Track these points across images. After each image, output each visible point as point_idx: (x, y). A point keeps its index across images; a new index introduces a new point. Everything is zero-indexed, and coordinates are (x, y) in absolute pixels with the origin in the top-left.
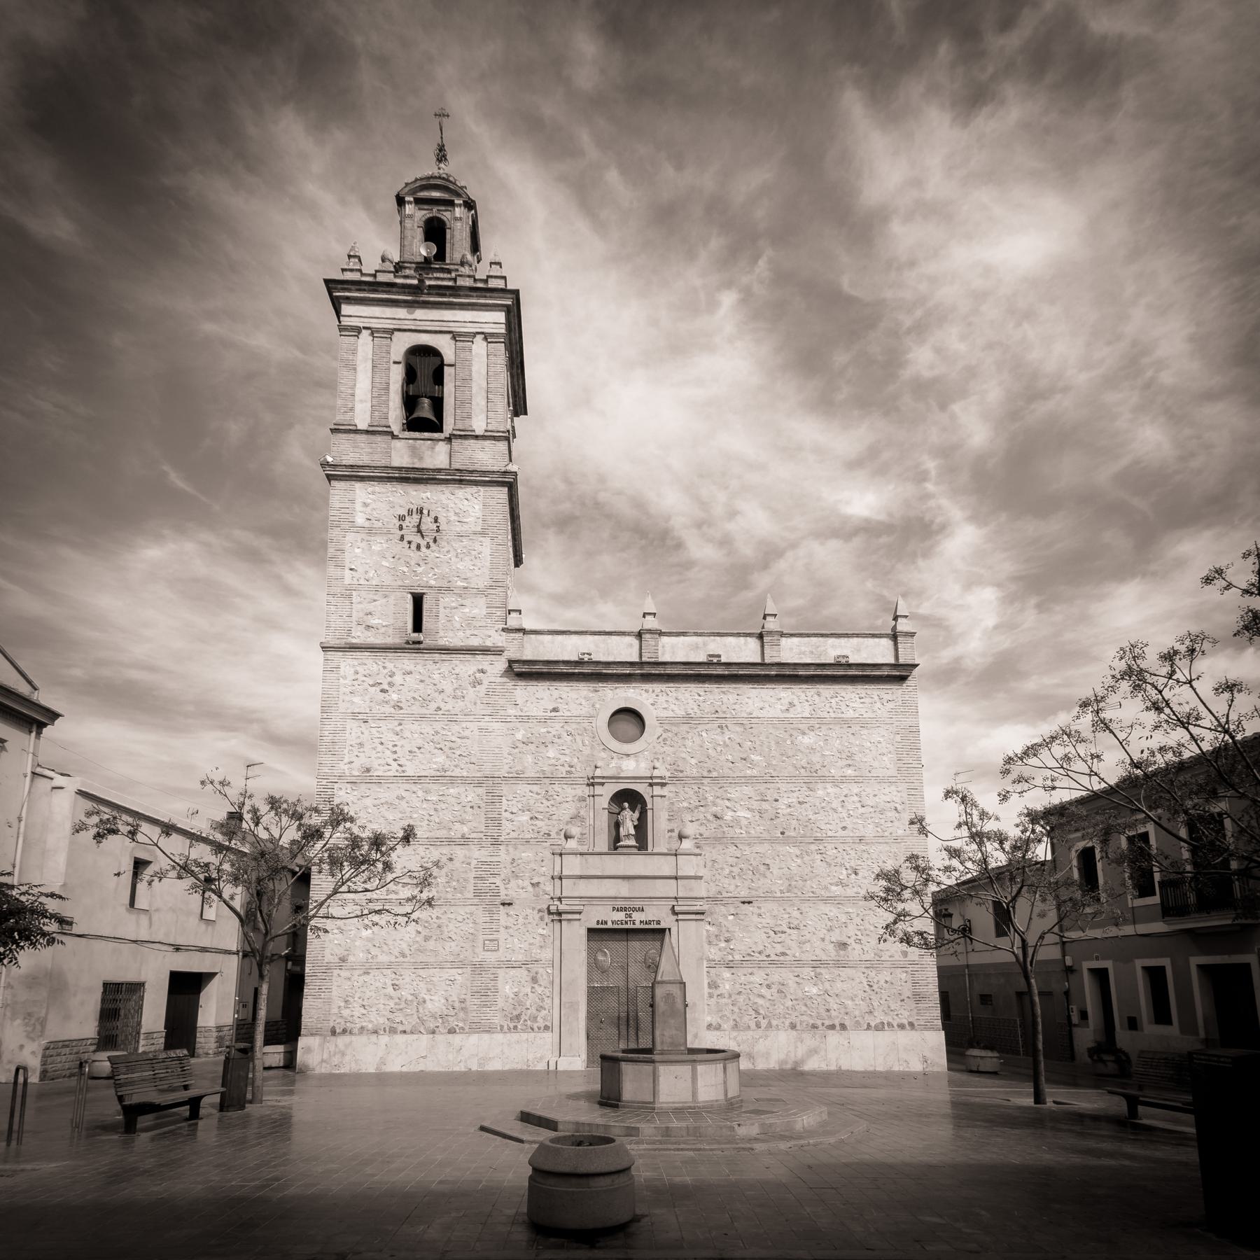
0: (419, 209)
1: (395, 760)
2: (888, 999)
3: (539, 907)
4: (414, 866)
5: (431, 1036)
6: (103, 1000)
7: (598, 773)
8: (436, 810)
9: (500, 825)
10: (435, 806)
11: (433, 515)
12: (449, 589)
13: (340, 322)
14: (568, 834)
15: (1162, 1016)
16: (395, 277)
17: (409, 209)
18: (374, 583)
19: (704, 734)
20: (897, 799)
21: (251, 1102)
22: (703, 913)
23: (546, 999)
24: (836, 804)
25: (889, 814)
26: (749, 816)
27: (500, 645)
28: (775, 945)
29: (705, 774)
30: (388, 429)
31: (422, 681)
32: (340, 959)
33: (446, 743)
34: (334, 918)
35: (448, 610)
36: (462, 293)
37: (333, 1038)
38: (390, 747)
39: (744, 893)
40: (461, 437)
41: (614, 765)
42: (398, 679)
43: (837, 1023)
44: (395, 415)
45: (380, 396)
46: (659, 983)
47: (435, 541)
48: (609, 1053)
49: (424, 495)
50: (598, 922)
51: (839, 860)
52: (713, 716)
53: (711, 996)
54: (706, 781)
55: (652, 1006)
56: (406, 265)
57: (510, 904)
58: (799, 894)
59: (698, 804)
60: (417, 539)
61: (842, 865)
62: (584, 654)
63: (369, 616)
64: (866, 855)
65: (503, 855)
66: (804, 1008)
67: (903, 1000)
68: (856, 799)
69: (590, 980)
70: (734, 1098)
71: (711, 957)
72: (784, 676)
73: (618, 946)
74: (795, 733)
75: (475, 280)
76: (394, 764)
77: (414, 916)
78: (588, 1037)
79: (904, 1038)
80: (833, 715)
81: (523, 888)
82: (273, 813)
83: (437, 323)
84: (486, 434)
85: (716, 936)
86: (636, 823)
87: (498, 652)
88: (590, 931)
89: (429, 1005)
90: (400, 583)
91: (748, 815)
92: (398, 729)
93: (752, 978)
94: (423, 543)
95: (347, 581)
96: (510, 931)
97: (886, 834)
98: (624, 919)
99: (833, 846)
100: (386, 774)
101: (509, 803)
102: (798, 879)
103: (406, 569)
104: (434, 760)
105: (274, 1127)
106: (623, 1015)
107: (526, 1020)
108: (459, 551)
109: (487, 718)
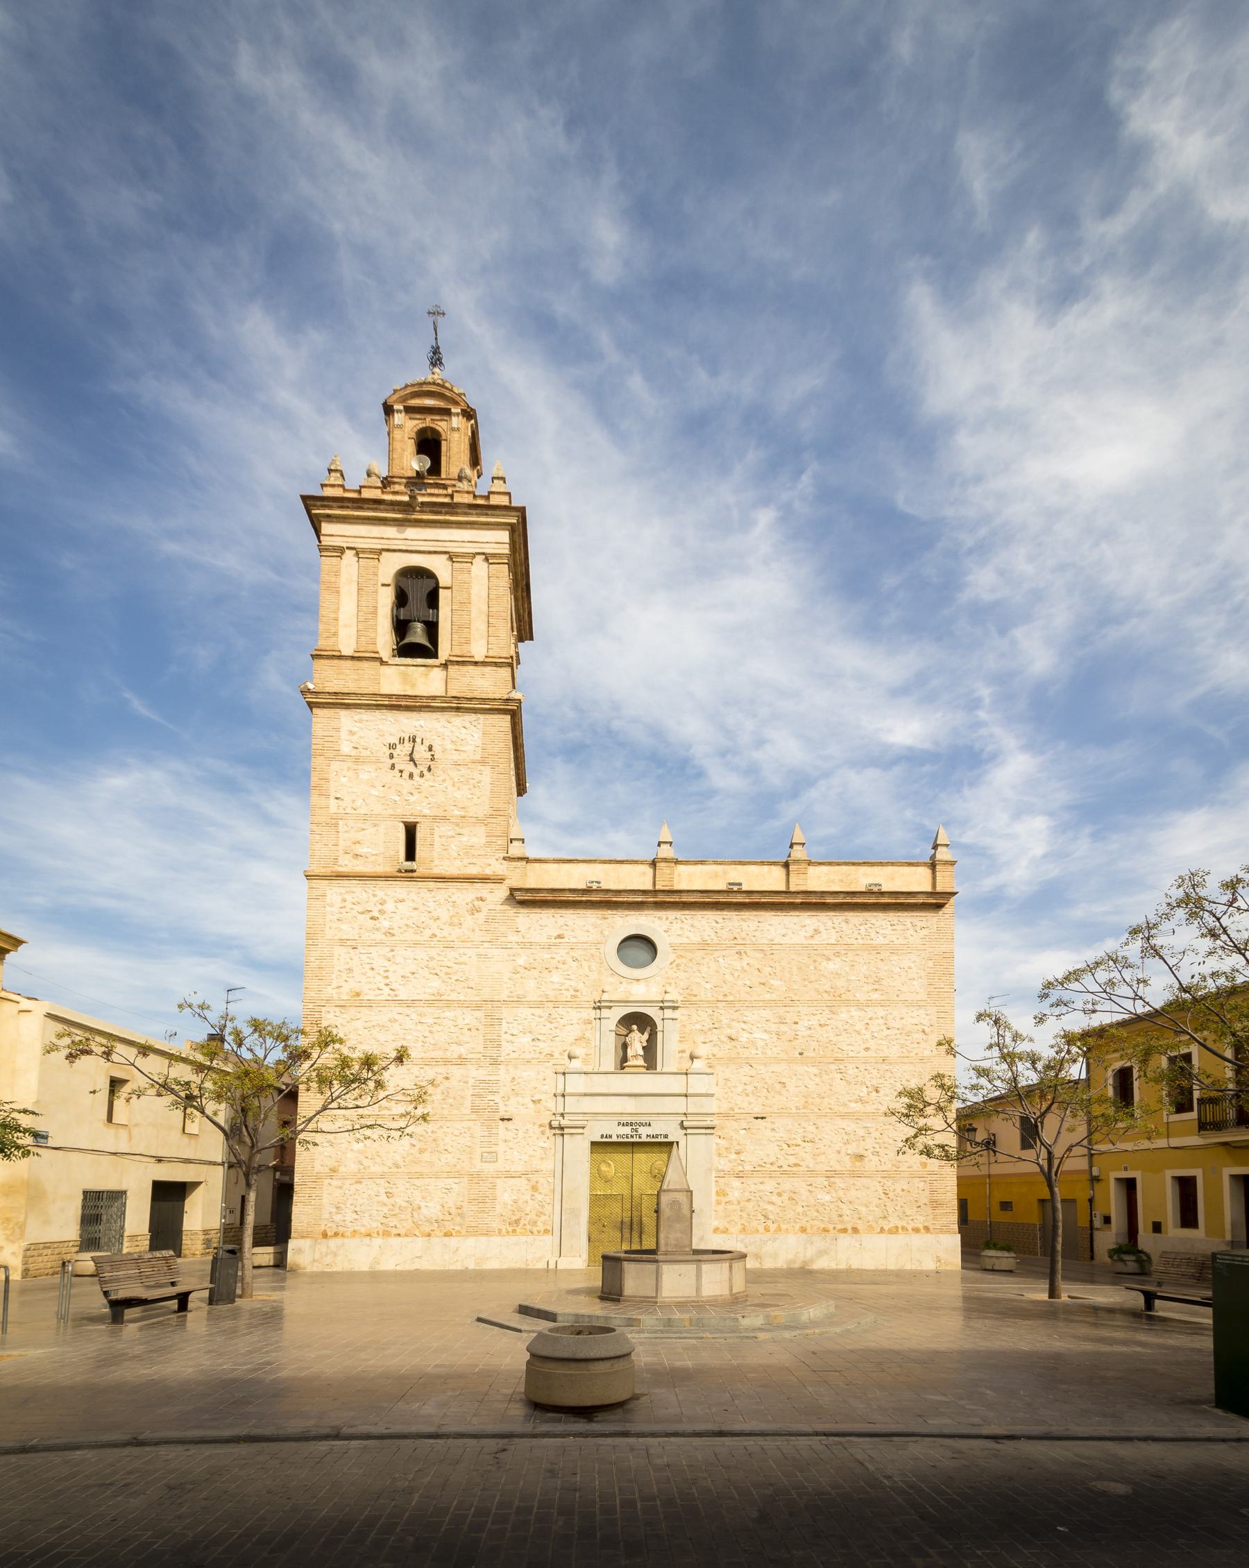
0: (410, 419)
1: (387, 985)
2: (904, 1205)
3: (540, 1123)
4: (408, 1084)
5: (427, 1238)
6: (84, 1207)
7: (605, 997)
8: (430, 1032)
9: (499, 1046)
10: (431, 1028)
11: (427, 743)
12: (445, 818)
13: (320, 542)
14: (572, 1055)
15: (1188, 1218)
16: (383, 492)
17: (399, 418)
18: (363, 811)
19: (720, 960)
20: (926, 1022)
21: (240, 1297)
22: (714, 1128)
23: (546, 1206)
24: (859, 1026)
25: (916, 1036)
26: (766, 1038)
27: (501, 873)
28: (787, 1156)
29: (721, 998)
30: (376, 655)
31: (415, 909)
32: (331, 1170)
33: (442, 968)
34: (324, 1132)
35: (444, 839)
36: (459, 511)
37: (324, 1240)
38: (382, 972)
39: (758, 1110)
40: (458, 663)
41: (621, 989)
42: (390, 906)
43: (849, 1227)
44: (385, 640)
45: (366, 620)
46: (665, 1191)
47: (429, 769)
48: (612, 1254)
49: (417, 724)
51: (860, 1079)
52: (732, 942)
53: (719, 1203)
54: (721, 1005)
55: (657, 1211)
56: (395, 480)
57: (509, 1120)
58: (816, 1110)
60: (410, 768)
61: (863, 1083)
62: (593, 882)
63: (358, 845)
64: (888, 1074)
65: (503, 1074)
66: (816, 1214)
68: (881, 1021)
69: (592, 1188)
70: (739, 1293)
71: (720, 1168)
72: (810, 904)
73: (623, 1158)
74: (819, 959)
75: (475, 496)
76: (386, 990)
77: (407, 1131)
78: (589, 1240)
79: (918, 1240)
80: (861, 942)
81: (523, 1105)
82: (256, 1035)
83: (431, 543)
84: (487, 660)
85: (727, 1149)
86: (645, 1044)
87: (499, 880)
88: (593, 1144)
89: (424, 1211)
90: (390, 812)
91: (765, 1036)
92: (390, 955)
93: (762, 1187)
94: (416, 772)
95: (333, 809)
96: (510, 1144)
97: (912, 1054)
99: (854, 1066)
100: (377, 998)
101: (511, 1025)
102: (815, 1096)
103: (397, 798)
104: (429, 985)
105: (264, 1319)
106: (627, 1220)
107: (525, 1225)
108: (456, 780)
109: (486, 945)
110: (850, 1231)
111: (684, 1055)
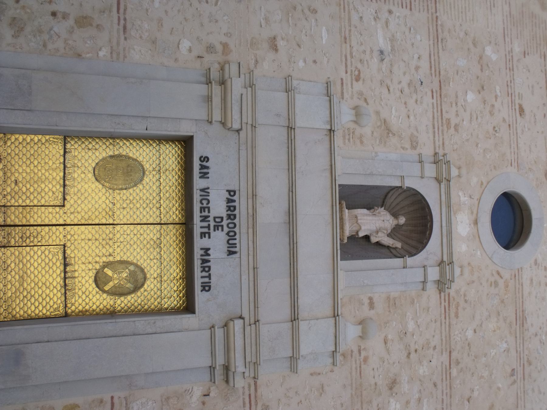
3: (232, 46)
41: (463, 199)
50: (207, 159)
54: (445, 358)
59: (412, 350)
81: (266, 19)
86: (374, 240)
98: (213, 214)
111: (366, 307)
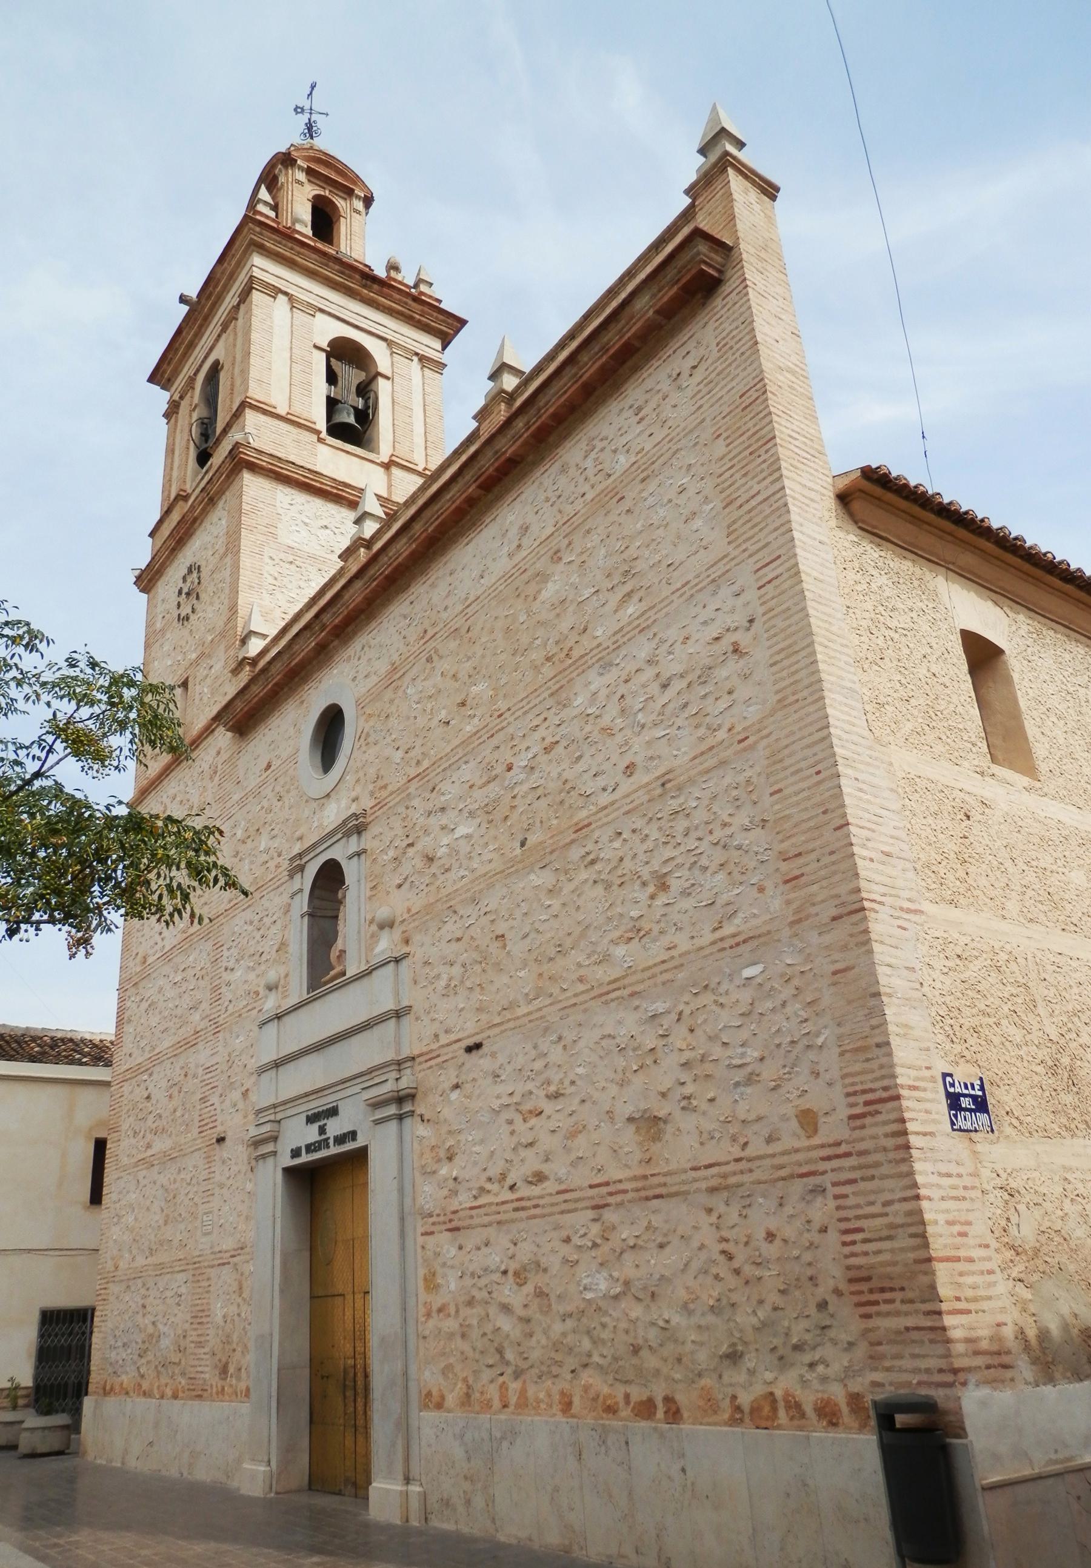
26: (470, 831)
67: (823, 1305)
110: (660, 1414)
